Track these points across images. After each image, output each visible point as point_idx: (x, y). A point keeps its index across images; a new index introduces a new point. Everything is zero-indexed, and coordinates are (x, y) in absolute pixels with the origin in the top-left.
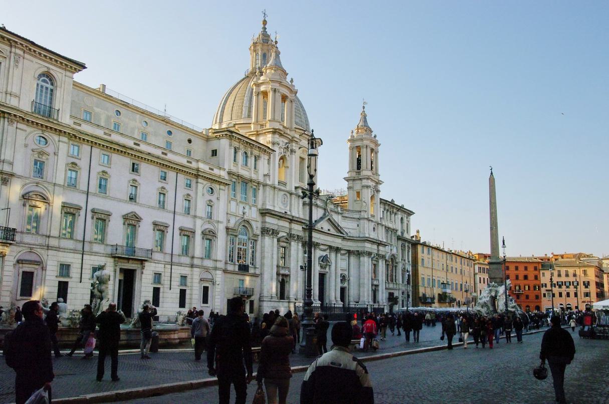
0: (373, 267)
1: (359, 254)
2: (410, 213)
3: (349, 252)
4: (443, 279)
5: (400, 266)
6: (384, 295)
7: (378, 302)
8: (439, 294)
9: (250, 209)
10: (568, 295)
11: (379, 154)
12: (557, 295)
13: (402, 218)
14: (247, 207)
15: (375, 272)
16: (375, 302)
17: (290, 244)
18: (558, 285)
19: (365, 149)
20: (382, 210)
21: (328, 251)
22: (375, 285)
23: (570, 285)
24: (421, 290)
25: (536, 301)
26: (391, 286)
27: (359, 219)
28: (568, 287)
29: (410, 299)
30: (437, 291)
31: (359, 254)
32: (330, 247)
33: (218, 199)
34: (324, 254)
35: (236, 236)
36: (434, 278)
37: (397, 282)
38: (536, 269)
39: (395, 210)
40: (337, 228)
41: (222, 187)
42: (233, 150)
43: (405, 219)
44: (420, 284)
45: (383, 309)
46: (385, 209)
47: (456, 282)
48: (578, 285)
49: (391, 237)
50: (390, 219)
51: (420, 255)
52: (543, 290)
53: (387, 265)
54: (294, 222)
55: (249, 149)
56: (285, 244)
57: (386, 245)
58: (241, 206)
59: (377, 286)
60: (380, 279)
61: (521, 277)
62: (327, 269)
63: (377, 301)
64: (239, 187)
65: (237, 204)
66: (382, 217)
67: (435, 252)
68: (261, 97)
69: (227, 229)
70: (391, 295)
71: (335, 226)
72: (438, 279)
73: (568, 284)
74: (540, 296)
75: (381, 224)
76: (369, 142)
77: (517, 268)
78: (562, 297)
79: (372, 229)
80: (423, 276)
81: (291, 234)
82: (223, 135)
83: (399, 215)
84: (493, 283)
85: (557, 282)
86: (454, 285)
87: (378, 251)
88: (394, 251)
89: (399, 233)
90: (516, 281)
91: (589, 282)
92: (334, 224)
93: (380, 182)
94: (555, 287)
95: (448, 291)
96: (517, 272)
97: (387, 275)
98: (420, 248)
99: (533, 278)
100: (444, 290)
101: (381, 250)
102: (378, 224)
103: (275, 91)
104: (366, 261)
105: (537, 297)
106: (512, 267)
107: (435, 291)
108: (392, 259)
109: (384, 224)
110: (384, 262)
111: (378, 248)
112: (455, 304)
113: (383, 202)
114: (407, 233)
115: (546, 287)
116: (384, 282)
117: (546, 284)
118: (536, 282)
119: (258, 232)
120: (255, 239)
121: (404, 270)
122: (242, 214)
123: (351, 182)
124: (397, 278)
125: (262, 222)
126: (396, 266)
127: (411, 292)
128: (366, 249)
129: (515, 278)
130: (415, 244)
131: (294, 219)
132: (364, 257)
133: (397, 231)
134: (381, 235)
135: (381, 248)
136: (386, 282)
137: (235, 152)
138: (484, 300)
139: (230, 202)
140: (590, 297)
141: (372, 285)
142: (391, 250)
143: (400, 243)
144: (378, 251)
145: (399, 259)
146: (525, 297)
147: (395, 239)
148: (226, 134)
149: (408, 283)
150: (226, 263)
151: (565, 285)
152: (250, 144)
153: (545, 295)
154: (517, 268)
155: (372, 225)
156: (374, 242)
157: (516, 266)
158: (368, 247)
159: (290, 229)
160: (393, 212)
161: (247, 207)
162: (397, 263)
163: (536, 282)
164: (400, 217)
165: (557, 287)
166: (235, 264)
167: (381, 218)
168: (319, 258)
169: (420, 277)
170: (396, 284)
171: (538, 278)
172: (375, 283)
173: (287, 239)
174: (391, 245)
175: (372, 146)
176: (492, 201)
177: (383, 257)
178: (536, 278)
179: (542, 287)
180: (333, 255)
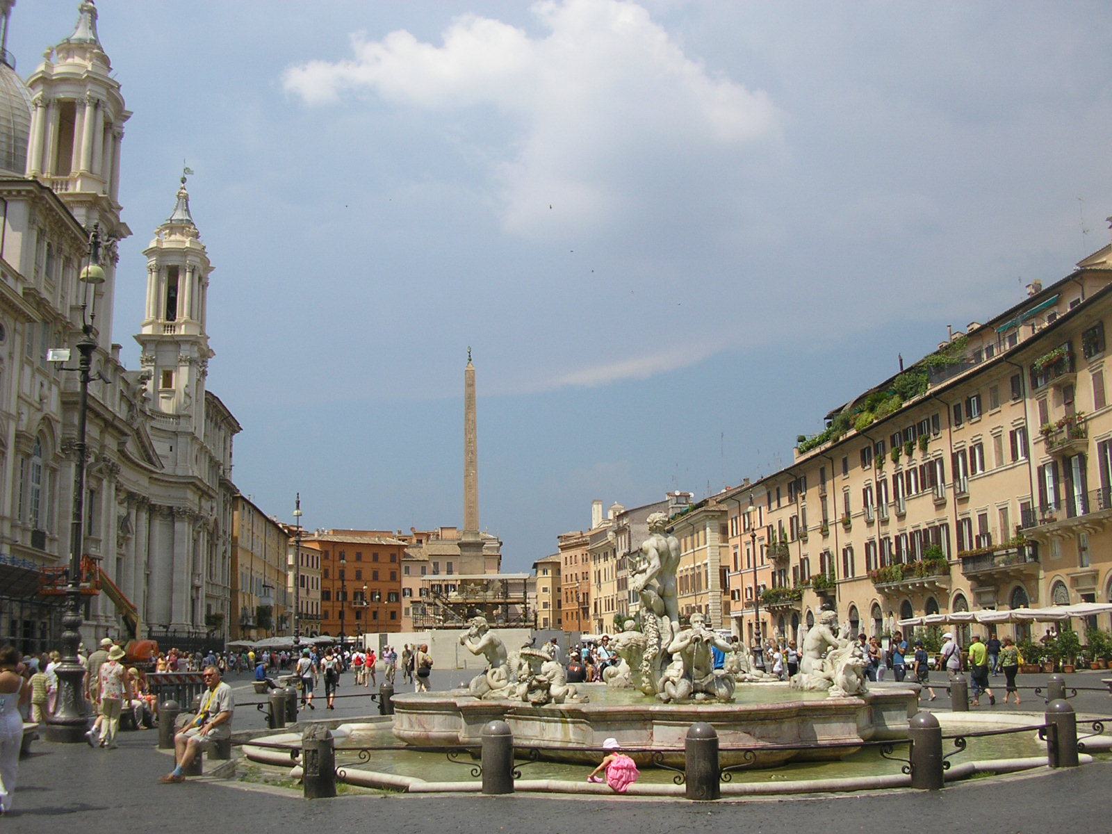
1: (172, 514)
2: (234, 427)
3: (153, 510)
5: (221, 549)
8: (258, 607)
9: (50, 389)
11: (209, 289)
14: (46, 383)
17: (100, 480)
19: (188, 274)
21: (126, 505)
25: (392, 622)
27: (175, 434)
30: (256, 602)
31: (172, 514)
32: (131, 496)
33: (11, 356)
34: (123, 512)
35: (28, 456)
38: (393, 559)
40: (146, 451)
41: (19, 327)
42: (35, 233)
44: (240, 587)
46: (207, 415)
52: (406, 602)
54: (110, 430)
55: (56, 238)
56: (93, 484)
58: (39, 378)
59: (198, 588)
61: (367, 574)
62: (124, 547)
64: (38, 331)
65: (33, 376)
68: (54, 114)
69: (19, 436)
70: (209, 607)
71: (143, 446)
76: (198, 260)
77: (359, 557)
81: (104, 459)
82: (19, 192)
87: (201, 508)
92: (142, 442)
93: (210, 354)
99: (388, 578)
103: (97, 105)
104: (184, 529)
111: (200, 499)
113: (213, 403)
115: (411, 595)
118: (393, 586)
119: (58, 450)
120: (55, 465)
122: (38, 400)
123: (151, 347)
125: (64, 425)
126: (216, 545)
128: (189, 504)
129: (354, 578)
130: (234, 498)
131: (117, 423)
132: (182, 520)
134: (200, 471)
135: (203, 502)
137: (38, 242)
139: (23, 366)
143: (222, 492)
144: (201, 508)
145: (221, 533)
146: (370, 616)
148: (29, 192)
150: (13, 526)
152: (64, 224)
153: (407, 609)
154: (359, 557)
155: (197, 447)
156: (199, 489)
157: (391, 554)
158: (191, 499)
159: (103, 447)
161: (46, 383)
163: (393, 586)
164: (222, 433)
166: (25, 530)
168: (119, 517)
171: (398, 576)
172: (197, 582)
173: (100, 471)
176: (471, 417)
178: (394, 577)
179: (404, 595)
180: (134, 512)
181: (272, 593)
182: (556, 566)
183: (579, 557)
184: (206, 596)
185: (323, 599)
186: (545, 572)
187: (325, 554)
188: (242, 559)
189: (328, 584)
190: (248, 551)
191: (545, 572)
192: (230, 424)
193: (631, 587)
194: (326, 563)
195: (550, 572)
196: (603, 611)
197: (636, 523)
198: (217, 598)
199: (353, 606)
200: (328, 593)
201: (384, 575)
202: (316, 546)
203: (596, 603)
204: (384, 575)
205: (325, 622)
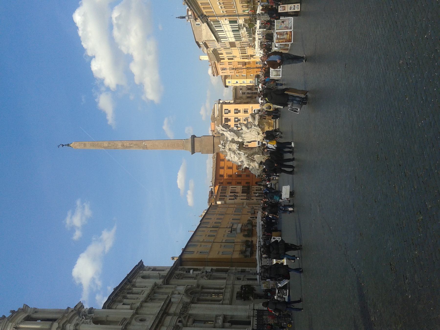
0: (195, 324)
2: (140, 266)
4: (227, 231)
5: (205, 282)
6: (240, 307)
7: (249, 317)
13: (144, 277)
15: (205, 322)
16: (248, 323)
20: (120, 306)
22: (224, 321)
24: (236, 255)
26: (228, 295)
29: (247, 269)
36: (224, 241)
37: (223, 287)
39: (128, 287)
43: (145, 273)
44: (229, 256)
45: (259, 311)
46: (120, 302)
47: (231, 219)
49: (163, 293)
50: (137, 294)
51: (196, 256)
53: (199, 301)
57: (170, 300)
59: (225, 319)
60: (215, 313)
63: (248, 320)
66: (129, 307)
67: (196, 238)
72: (226, 236)
75: (136, 310)
79: (141, 323)
80: (221, 253)
83: (138, 281)
84: (220, 146)
86: (234, 221)
88: (182, 289)
89: (159, 281)
91: (235, 109)
93: (78, 307)
95: (240, 226)
97: (212, 301)
98: (187, 256)
100: (239, 231)
101: (174, 310)
102: (137, 313)
107: (239, 240)
108: (191, 293)
109: (138, 304)
110: (193, 305)
111: (168, 314)
112: (254, 221)
114: (163, 270)
116: (221, 306)
121: (210, 277)
124: (218, 287)
126: (203, 288)
127: (238, 268)
130: (181, 262)
133: (156, 285)
134: (153, 309)
135: (172, 310)
136: (222, 304)
138: (243, 158)
140: (248, 109)
141: (223, 327)
142: (179, 294)
144: (175, 314)
147: (166, 288)
149: (226, 271)
156: (160, 322)
160: (130, 289)
162: (198, 286)
167: (131, 309)
169: (220, 256)
170: (226, 287)
172: (220, 322)
174: (173, 293)
175: (23, 316)
177: (186, 307)
181: (235, 226)
182: (226, 77)
183: (221, 66)
184: (231, 304)
188: (213, 255)
190: (212, 245)
192: (134, 273)
193: (233, 40)
196: (247, 55)
197: (202, 37)
198: (234, 284)
202: (217, 187)
203: (243, 59)
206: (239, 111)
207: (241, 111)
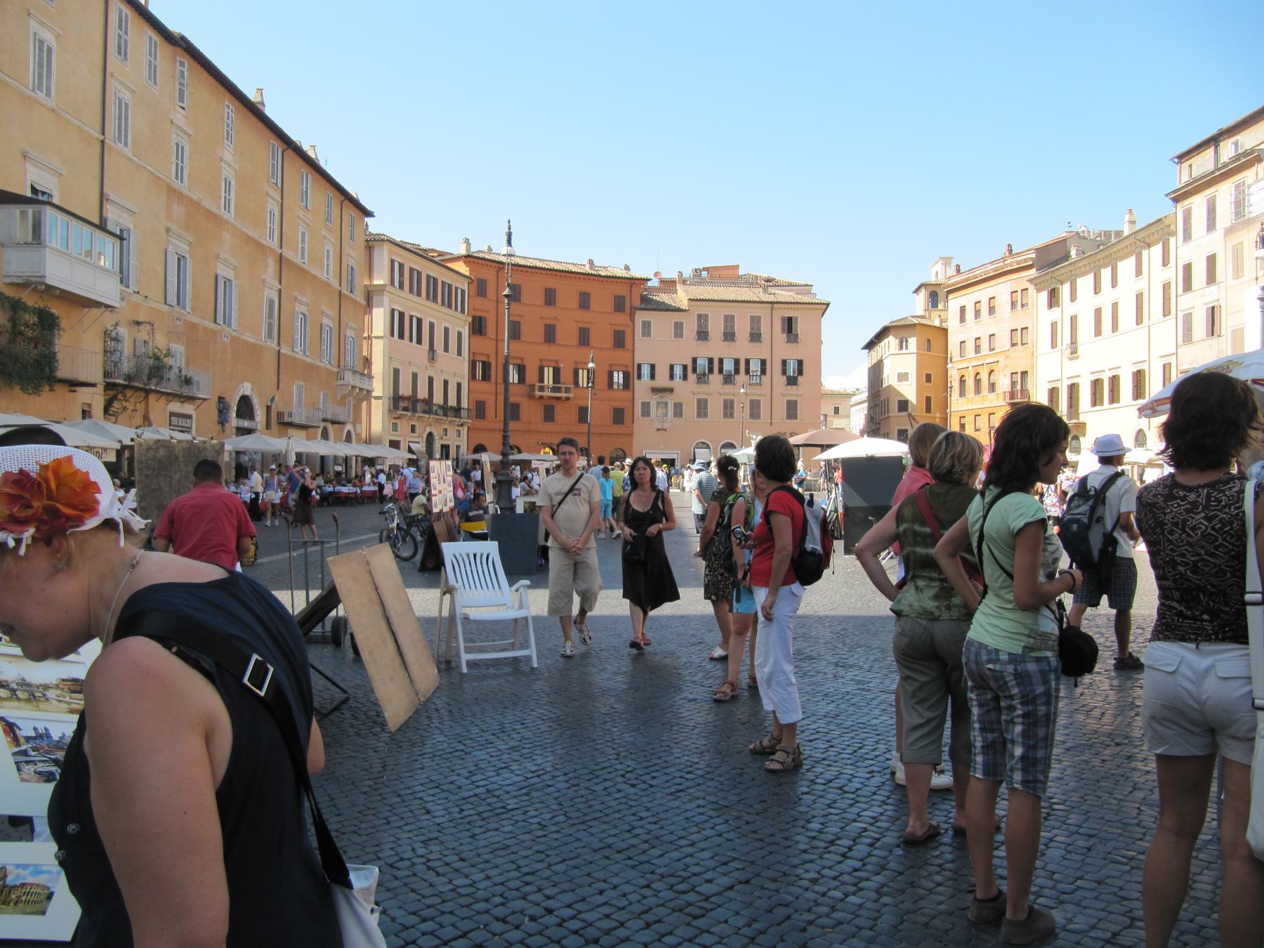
10: (728, 408)
12: (690, 410)
18: (694, 370)
23: (737, 371)
25: (616, 429)
28: (728, 379)
38: (619, 304)
48: (763, 372)
52: (642, 387)
73: (728, 366)
74: (627, 415)
78: (732, 416)
85: (695, 360)
90: (545, 348)
91: (800, 363)
94: (685, 377)
96: (549, 312)
105: (619, 416)
106: (533, 292)
115: (653, 377)
117: (653, 367)
129: (541, 339)
151: (721, 371)
163: (620, 356)
165: (692, 377)
178: (620, 340)
183: (1003, 301)
185: (473, 376)
186: (902, 344)
187: (481, 288)
189: (485, 345)
191: (902, 344)
194: (481, 303)
195: (913, 342)
199: (538, 393)
200: (486, 366)
201: (602, 335)
204: (602, 335)
205: (480, 424)
206: (792, 381)
207: (792, 390)
